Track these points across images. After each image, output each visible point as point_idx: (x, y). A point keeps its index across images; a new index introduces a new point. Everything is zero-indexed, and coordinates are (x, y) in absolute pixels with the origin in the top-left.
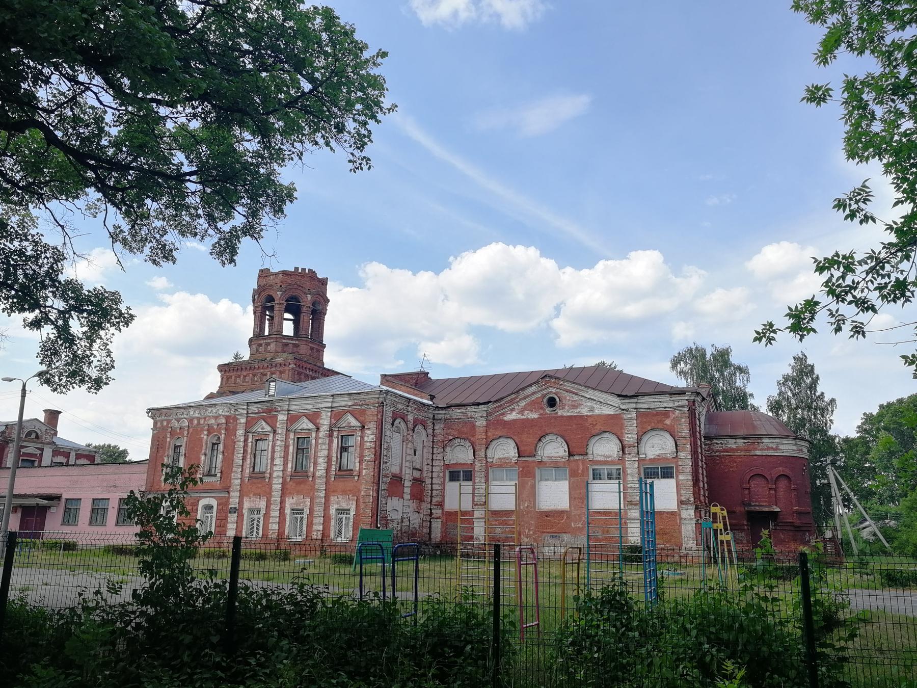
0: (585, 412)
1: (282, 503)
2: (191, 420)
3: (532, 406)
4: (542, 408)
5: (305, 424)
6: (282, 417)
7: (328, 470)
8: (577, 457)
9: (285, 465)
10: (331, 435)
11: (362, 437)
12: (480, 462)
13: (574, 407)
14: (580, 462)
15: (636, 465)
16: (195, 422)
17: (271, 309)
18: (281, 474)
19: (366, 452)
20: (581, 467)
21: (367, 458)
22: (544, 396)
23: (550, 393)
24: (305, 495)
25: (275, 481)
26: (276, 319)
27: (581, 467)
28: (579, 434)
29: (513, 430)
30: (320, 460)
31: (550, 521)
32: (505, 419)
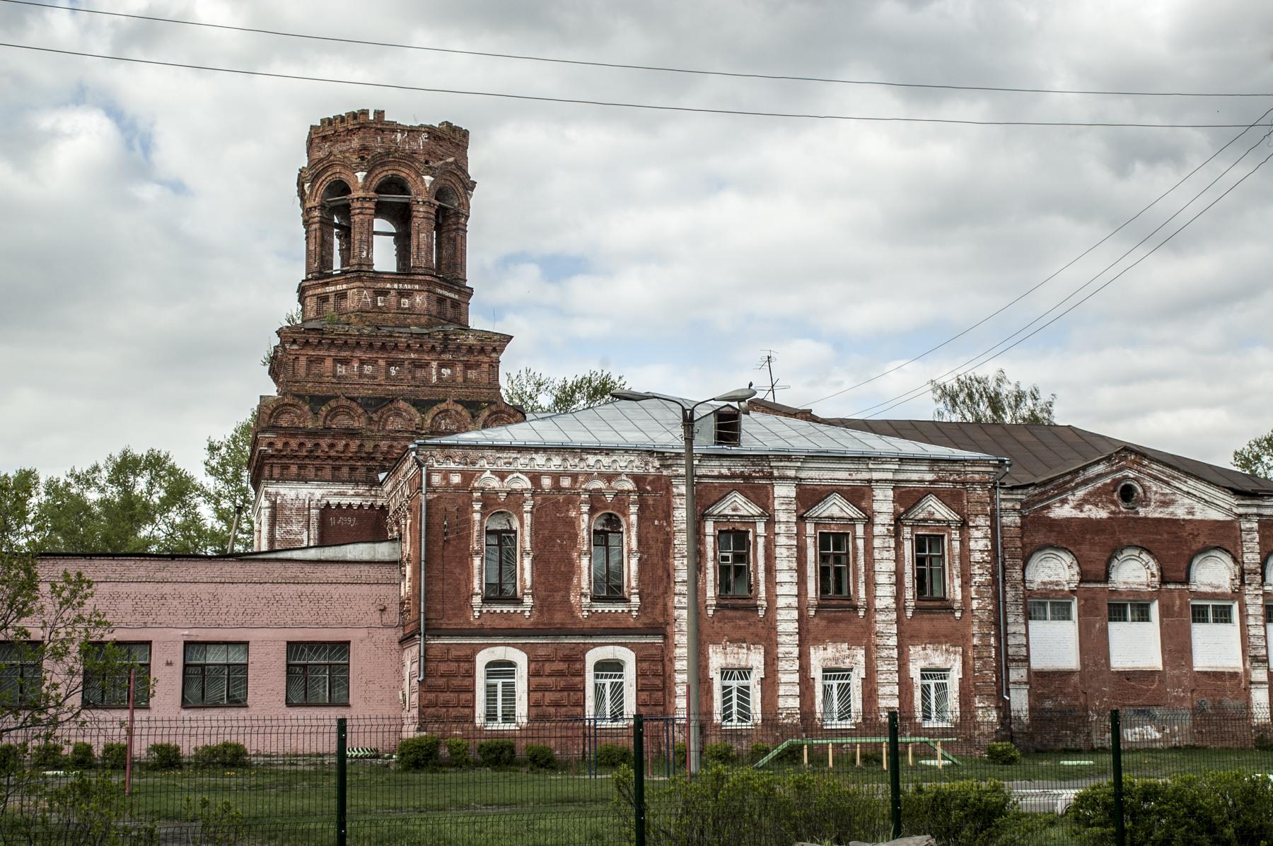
0: (1180, 513)
1: (803, 657)
2: (535, 477)
3: (1093, 499)
4: (1114, 502)
5: (836, 507)
6: (784, 492)
7: (899, 597)
8: (1172, 587)
9: (802, 582)
10: (897, 534)
11: (964, 543)
12: (1014, 587)
13: (1165, 504)
14: (1176, 594)
15: (1260, 601)
16: (546, 482)
17: (345, 210)
18: (794, 602)
19: (976, 570)
20: (1178, 602)
21: (977, 579)
22: (1116, 482)
23: (1126, 478)
24: (854, 642)
25: (782, 615)
26: (356, 236)
27: (1178, 602)
28: (1176, 547)
29: (1067, 537)
30: (881, 579)
31: (1133, 687)
32: (1052, 515)
